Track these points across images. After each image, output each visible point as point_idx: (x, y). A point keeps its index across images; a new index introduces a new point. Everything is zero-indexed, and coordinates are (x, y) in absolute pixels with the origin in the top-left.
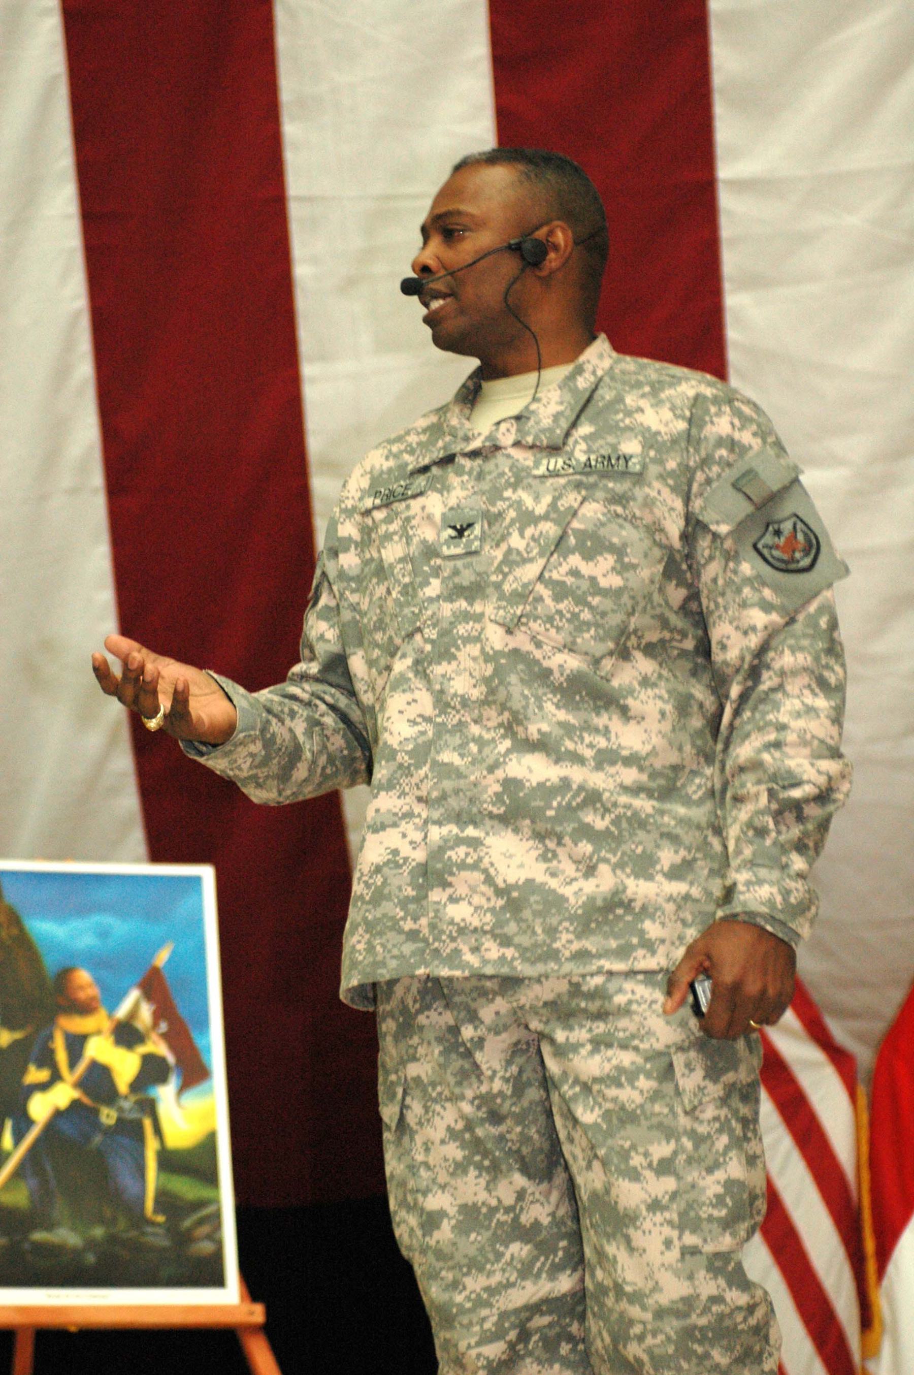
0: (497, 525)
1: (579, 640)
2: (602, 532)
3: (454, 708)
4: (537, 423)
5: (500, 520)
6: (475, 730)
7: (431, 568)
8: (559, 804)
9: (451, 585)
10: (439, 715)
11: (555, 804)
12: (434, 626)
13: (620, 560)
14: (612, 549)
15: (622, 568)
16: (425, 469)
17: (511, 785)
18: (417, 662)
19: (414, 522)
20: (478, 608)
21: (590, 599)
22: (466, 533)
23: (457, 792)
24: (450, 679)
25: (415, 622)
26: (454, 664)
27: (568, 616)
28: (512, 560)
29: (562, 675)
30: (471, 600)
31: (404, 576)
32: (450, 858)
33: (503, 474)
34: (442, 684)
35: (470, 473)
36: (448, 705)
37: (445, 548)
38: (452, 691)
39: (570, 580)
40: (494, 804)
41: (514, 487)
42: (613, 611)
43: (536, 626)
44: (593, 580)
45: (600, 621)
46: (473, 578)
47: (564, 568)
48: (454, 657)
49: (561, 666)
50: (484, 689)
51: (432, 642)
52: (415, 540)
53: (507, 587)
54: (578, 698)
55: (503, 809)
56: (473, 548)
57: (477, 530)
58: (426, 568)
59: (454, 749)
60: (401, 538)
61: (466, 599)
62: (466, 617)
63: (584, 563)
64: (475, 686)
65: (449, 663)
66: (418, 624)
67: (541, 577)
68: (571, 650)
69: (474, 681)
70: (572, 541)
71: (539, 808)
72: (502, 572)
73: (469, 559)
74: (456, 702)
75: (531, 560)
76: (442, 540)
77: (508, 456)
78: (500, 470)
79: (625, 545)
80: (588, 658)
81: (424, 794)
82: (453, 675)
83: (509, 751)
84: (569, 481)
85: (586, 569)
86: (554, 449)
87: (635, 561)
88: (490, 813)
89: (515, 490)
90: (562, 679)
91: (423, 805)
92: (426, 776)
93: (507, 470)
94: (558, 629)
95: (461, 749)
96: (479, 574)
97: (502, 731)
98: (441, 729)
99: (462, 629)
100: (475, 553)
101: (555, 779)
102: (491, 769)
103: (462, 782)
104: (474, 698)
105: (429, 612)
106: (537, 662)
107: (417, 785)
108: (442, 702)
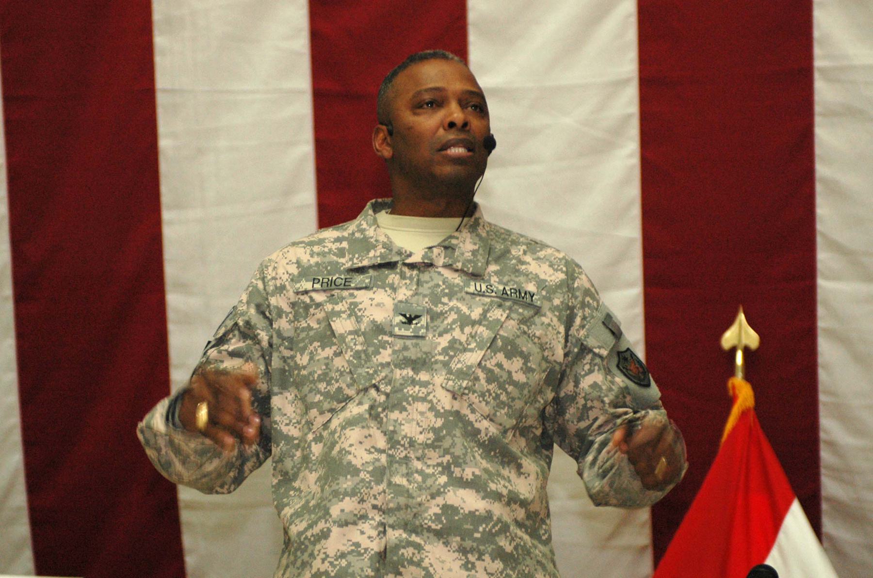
0: (439, 320)
1: (498, 414)
2: (518, 341)
3: (403, 446)
4: (463, 254)
5: (442, 318)
6: (418, 465)
7: (379, 341)
8: (484, 529)
9: (401, 357)
10: (390, 449)
11: (481, 529)
12: (389, 383)
13: (525, 364)
14: (522, 354)
15: (527, 370)
16: (361, 270)
17: (447, 509)
18: (372, 407)
19: (360, 307)
20: (423, 376)
21: (507, 386)
22: (414, 322)
23: (407, 506)
24: (401, 424)
25: (371, 380)
26: (405, 414)
27: (494, 395)
28: (455, 347)
29: (486, 435)
30: (416, 370)
31: (355, 344)
32: (403, 554)
33: (438, 285)
34: (395, 426)
35: (411, 278)
36: (398, 443)
37: (396, 329)
38: (403, 433)
39: (497, 370)
40: (433, 522)
41: (450, 296)
42: (519, 398)
43: (474, 398)
44: (510, 373)
45: (511, 404)
46: (419, 355)
47: (494, 361)
48: (405, 409)
49: (487, 429)
50: (431, 435)
51: (387, 395)
52: (365, 320)
53: (453, 366)
54: (492, 453)
55: (440, 526)
56: (420, 334)
57: (424, 321)
58: (376, 341)
59: (403, 475)
60: (350, 316)
61: (413, 369)
62: (414, 382)
63: (506, 360)
64: (421, 433)
65: (401, 412)
66: (374, 382)
67: (480, 364)
68: (491, 420)
69: (421, 429)
70: (499, 343)
71: (469, 529)
72: (448, 354)
73: (414, 341)
74: (406, 442)
75: (472, 350)
76: (394, 323)
77: (439, 273)
78: (435, 282)
79: (529, 354)
80: (501, 427)
81: (378, 503)
82: (403, 422)
83: (445, 485)
84: (492, 301)
85: (506, 364)
86: (476, 276)
87: (533, 366)
88: (430, 527)
89: (450, 300)
90: (486, 438)
91: (376, 511)
92: (384, 492)
93: (441, 283)
94: (487, 403)
95: (408, 475)
96: (426, 353)
97: (440, 469)
98: (391, 459)
99: (410, 390)
100: (423, 337)
101: (482, 511)
102: (433, 496)
103: (411, 500)
104: (420, 441)
105: (383, 374)
106: (471, 424)
107: (375, 496)
108: (392, 439)
